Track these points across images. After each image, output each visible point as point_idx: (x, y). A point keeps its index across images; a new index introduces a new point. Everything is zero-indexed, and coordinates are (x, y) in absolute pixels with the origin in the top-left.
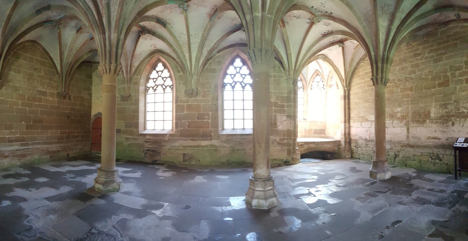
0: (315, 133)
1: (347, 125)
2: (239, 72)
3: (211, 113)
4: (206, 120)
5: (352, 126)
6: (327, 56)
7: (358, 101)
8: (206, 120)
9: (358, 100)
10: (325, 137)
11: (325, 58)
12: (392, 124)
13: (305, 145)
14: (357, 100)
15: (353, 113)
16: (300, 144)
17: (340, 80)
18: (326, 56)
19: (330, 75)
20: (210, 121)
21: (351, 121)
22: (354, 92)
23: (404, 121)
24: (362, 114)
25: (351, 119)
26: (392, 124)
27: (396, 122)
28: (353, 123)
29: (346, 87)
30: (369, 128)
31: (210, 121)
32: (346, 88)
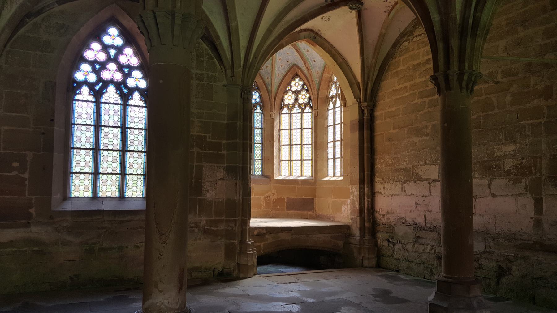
0: (288, 208)
1: (366, 189)
2: (115, 60)
3: (30, 155)
4: (14, 173)
5: (378, 192)
6: (319, 33)
7: (395, 131)
8: (14, 173)
9: (394, 129)
10: (314, 215)
11: (314, 38)
12: (489, 188)
13: (267, 236)
14: (392, 131)
15: (382, 161)
16: (256, 232)
17: (351, 85)
18: (316, 34)
19: (325, 75)
20: (26, 175)
21: (377, 179)
22: (383, 112)
23: (524, 181)
24: (405, 163)
25: (377, 174)
26: (489, 188)
27: (499, 182)
28: (382, 183)
29: (365, 100)
30: (424, 198)
31: (26, 175)
32: (364, 104)
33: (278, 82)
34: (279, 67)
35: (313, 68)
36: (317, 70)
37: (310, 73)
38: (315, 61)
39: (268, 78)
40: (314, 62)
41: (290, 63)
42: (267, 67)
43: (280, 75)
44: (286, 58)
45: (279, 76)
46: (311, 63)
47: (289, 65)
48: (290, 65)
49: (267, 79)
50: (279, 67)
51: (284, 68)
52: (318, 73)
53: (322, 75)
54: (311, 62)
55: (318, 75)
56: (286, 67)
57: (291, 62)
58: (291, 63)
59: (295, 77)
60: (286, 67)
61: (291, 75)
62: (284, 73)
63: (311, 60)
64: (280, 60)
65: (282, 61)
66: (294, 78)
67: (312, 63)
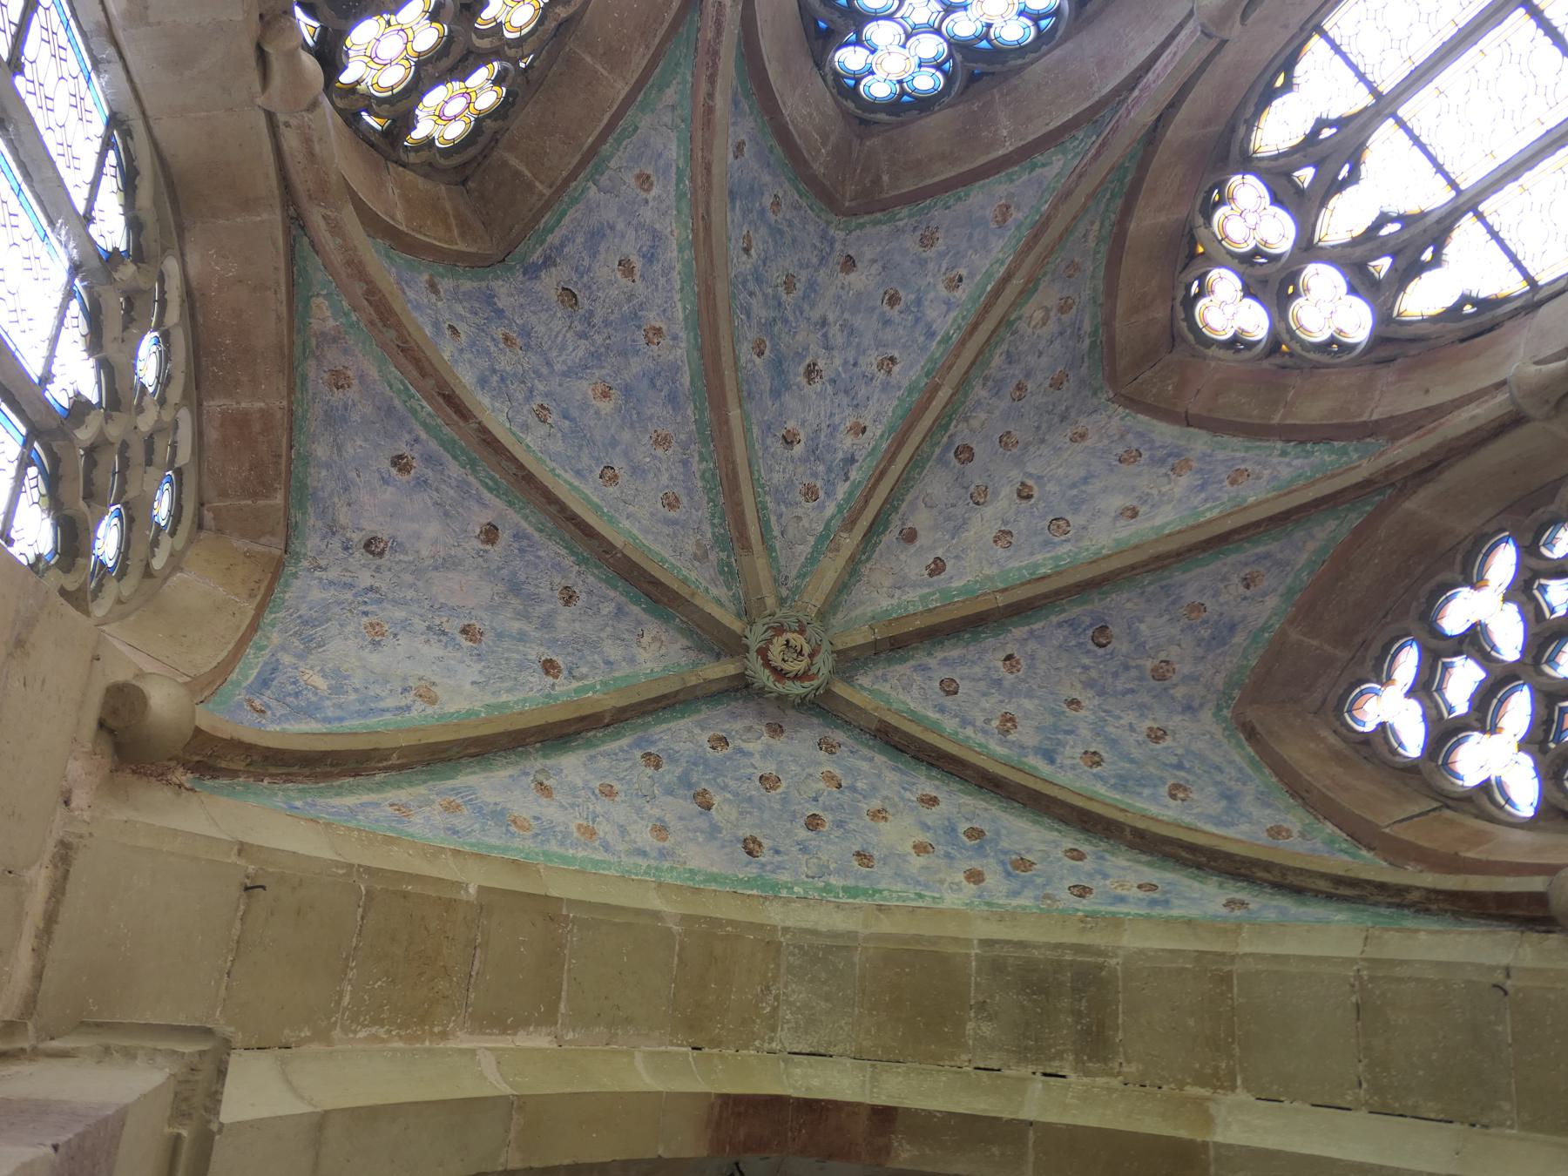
33: (645, 122)
34: (650, 258)
35: (397, 402)
36: (352, 394)
37: (424, 375)
38: (400, 463)
39: (739, 147)
40: (403, 449)
41: (549, 284)
42: (747, 250)
43: (630, 179)
44: (599, 339)
45: (645, 181)
46: (423, 435)
47: (548, 262)
48: (536, 256)
49: (744, 137)
50: (657, 267)
51: (596, 236)
52: (336, 373)
53: (294, 382)
54: (433, 445)
55: (333, 357)
56: (580, 239)
57: (538, 286)
58: (532, 271)
59: (472, 151)
60: (580, 239)
61: (517, 174)
62: (593, 191)
63: (429, 459)
64: (658, 331)
65: (635, 316)
66: (482, 140)
67: (416, 440)
